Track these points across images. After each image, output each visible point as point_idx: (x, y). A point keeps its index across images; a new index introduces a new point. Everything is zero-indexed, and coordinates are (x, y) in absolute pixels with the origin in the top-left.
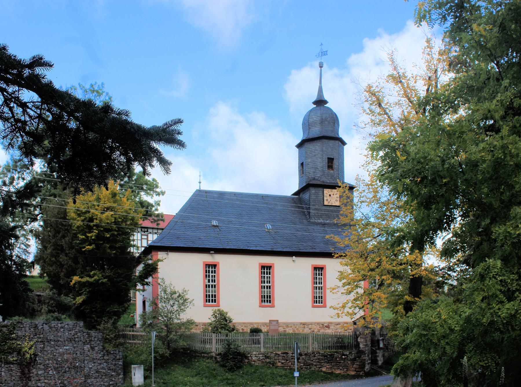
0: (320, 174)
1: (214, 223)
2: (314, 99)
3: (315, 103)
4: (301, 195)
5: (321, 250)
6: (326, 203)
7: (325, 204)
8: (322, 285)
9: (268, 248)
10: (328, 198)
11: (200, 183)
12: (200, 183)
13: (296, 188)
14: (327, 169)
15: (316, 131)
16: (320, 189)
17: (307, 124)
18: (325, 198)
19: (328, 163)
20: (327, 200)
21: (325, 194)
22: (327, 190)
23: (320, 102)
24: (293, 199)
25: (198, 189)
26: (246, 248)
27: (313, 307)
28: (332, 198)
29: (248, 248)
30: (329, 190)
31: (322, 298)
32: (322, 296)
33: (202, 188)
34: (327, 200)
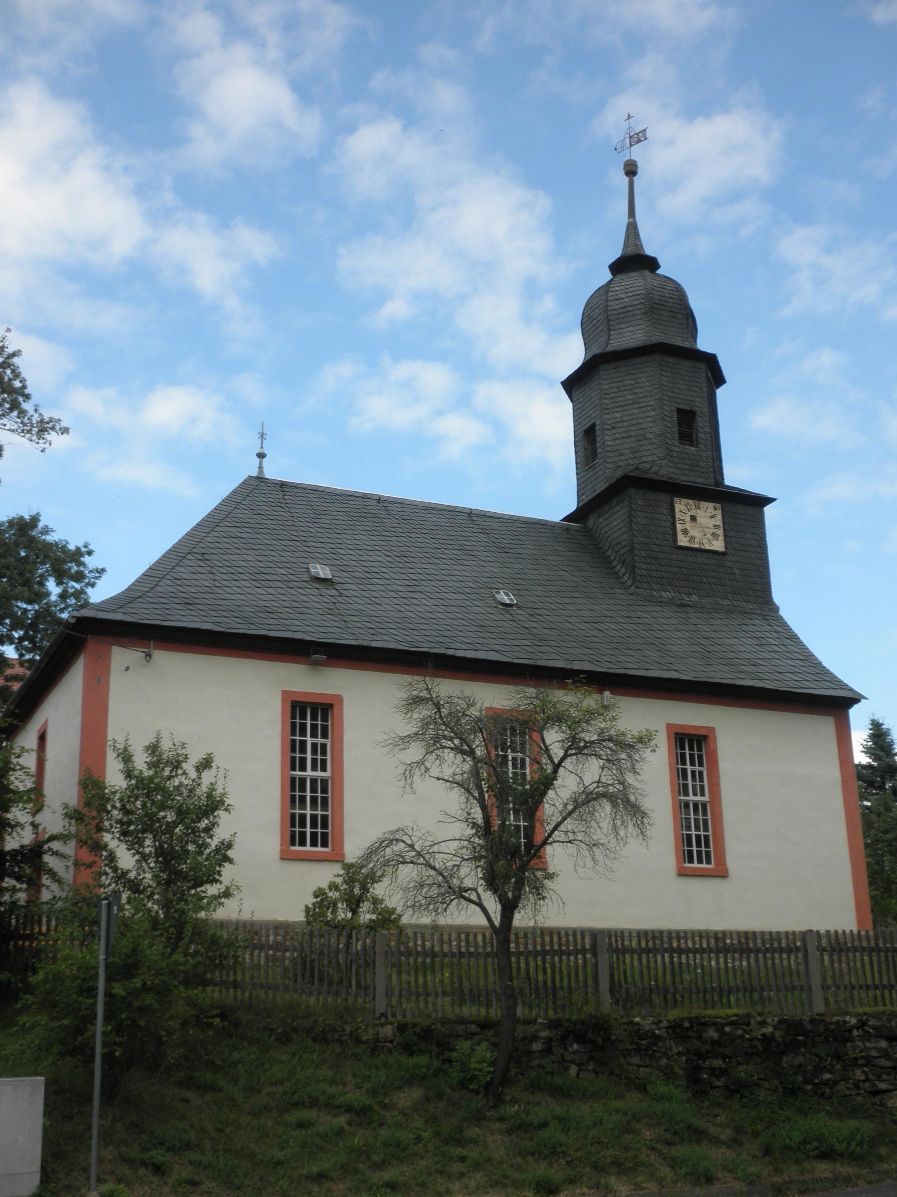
0: (657, 459)
1: (323, 572)
2: (616, 253)
3: (617, 268)
4: (591, 522)
5: (696, 674)
6: (683, 541)
7: (680, 543)
8: (706, 798)
9: (520, 656)
10: (689, 525)
11: (261, 456)
12: (261, 456)
13: (570, 505)
14: (676, 442)
15: (633, 335)
16: (663, 497)
17: (597, 317)
18: (679, 527)
19: (680, 424)
20: (685, 532)
21: (678, 515)
22: (684, 501)
23: (634, 262)
24: (568, 529)
25: (255, 475)
26: (443, 651)
27: (682, 873)
28: (700, 527)
29: (450, 652)
30: (691, 502)
31: (707, 845)
32: (707, 838)
33: (272, 472)
34: (685, 532)
